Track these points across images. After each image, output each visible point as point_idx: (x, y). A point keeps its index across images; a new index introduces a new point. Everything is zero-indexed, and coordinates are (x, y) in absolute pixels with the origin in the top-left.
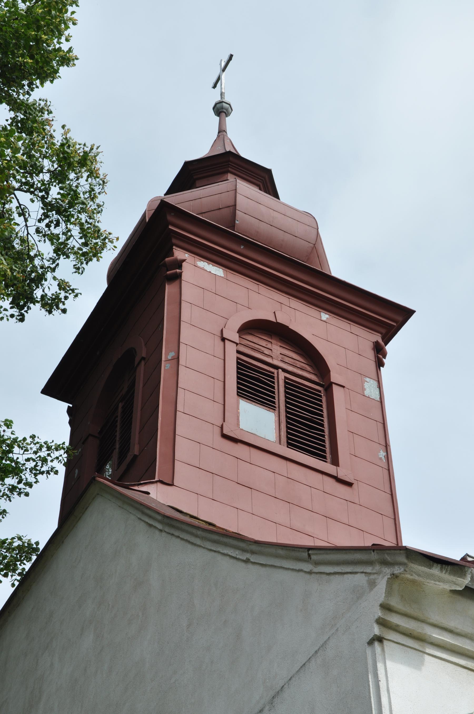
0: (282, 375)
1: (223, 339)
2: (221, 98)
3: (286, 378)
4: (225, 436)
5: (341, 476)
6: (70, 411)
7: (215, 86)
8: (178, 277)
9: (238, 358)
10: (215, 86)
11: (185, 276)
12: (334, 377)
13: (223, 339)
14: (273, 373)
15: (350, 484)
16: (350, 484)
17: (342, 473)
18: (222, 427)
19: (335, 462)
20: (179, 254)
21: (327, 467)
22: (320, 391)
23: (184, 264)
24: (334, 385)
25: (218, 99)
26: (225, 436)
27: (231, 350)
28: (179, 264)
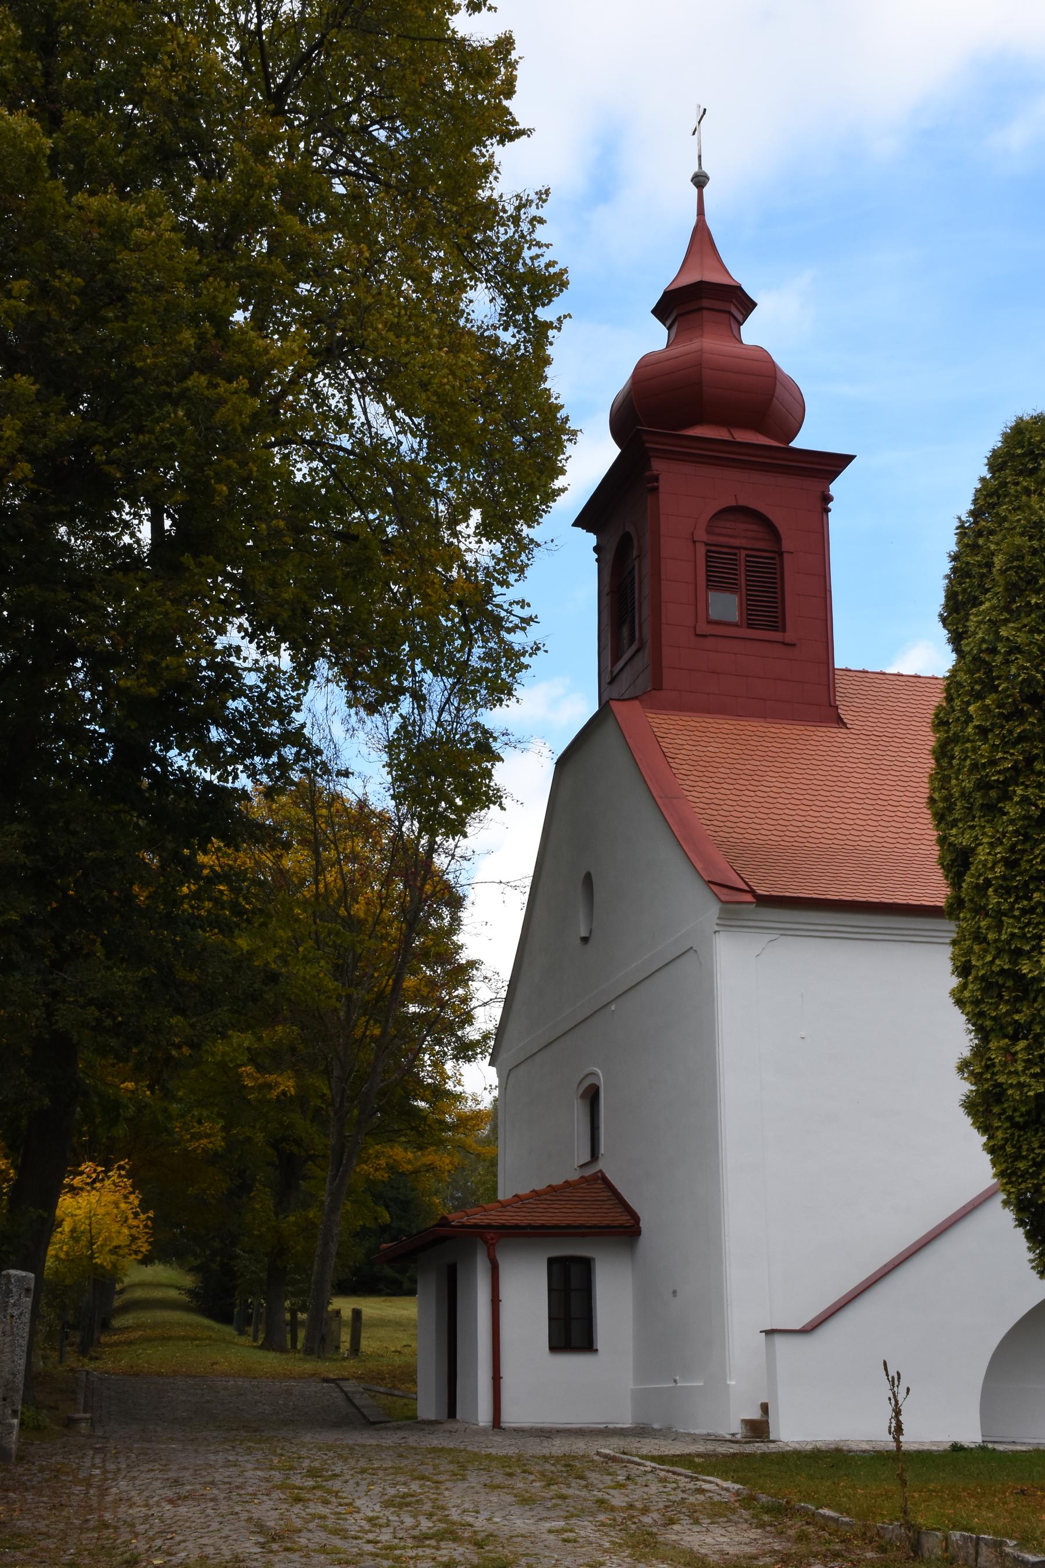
0: (744, 553)
1: (694, 542)
2: (700, 164)
3: (747, 556)
4: (697, 635)
5: (787, 641)
6: (596, 549)
7: (694, 134)
8: (656, 489)
9: (708, 551)
10: (694, 134)
11: (661, 489)
12: (786, 545)
13: (694, 542)
14: (735, 555)
15: (794, 645)
16: (794, 645)
17: (789, 636)
18: (695, 627)
19: (784, 631)
20: (658, 466)
21: (777, 636)
22: (773, 558)
23: (661, 478)
24: (785, 555)
25: (696, 169)
26: (697, 635)
27: (701, 550)
28: (656, 479)
